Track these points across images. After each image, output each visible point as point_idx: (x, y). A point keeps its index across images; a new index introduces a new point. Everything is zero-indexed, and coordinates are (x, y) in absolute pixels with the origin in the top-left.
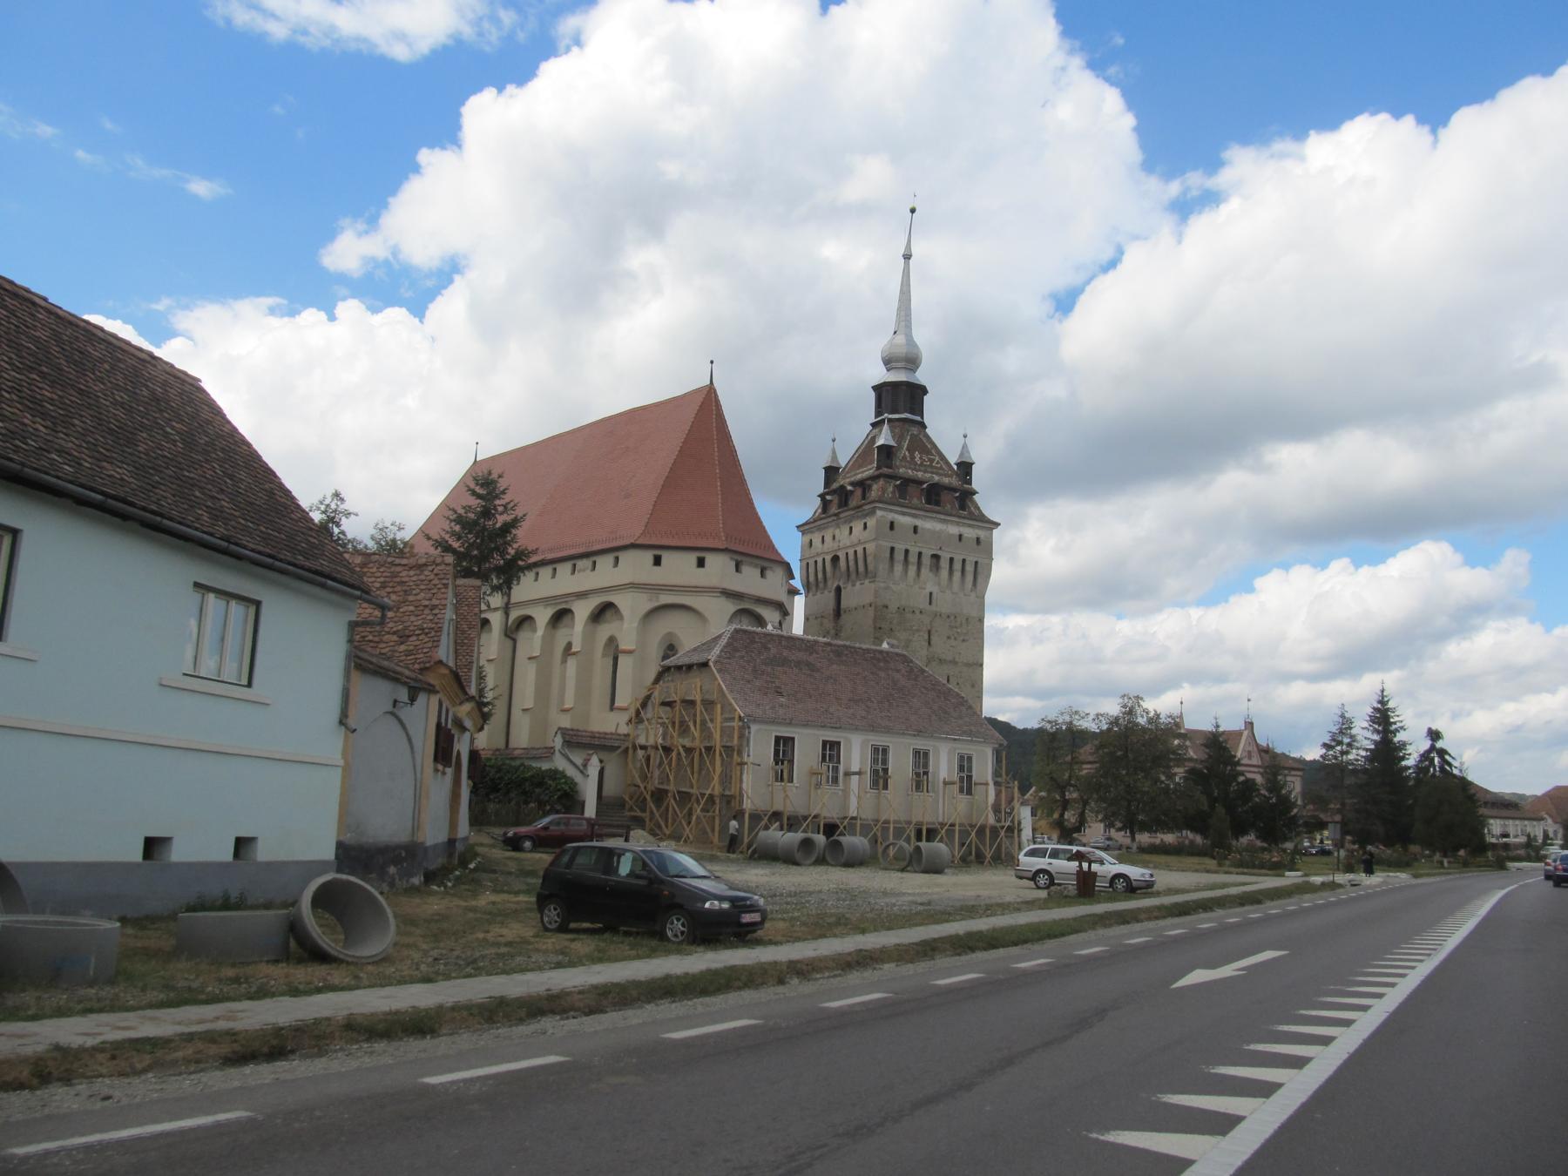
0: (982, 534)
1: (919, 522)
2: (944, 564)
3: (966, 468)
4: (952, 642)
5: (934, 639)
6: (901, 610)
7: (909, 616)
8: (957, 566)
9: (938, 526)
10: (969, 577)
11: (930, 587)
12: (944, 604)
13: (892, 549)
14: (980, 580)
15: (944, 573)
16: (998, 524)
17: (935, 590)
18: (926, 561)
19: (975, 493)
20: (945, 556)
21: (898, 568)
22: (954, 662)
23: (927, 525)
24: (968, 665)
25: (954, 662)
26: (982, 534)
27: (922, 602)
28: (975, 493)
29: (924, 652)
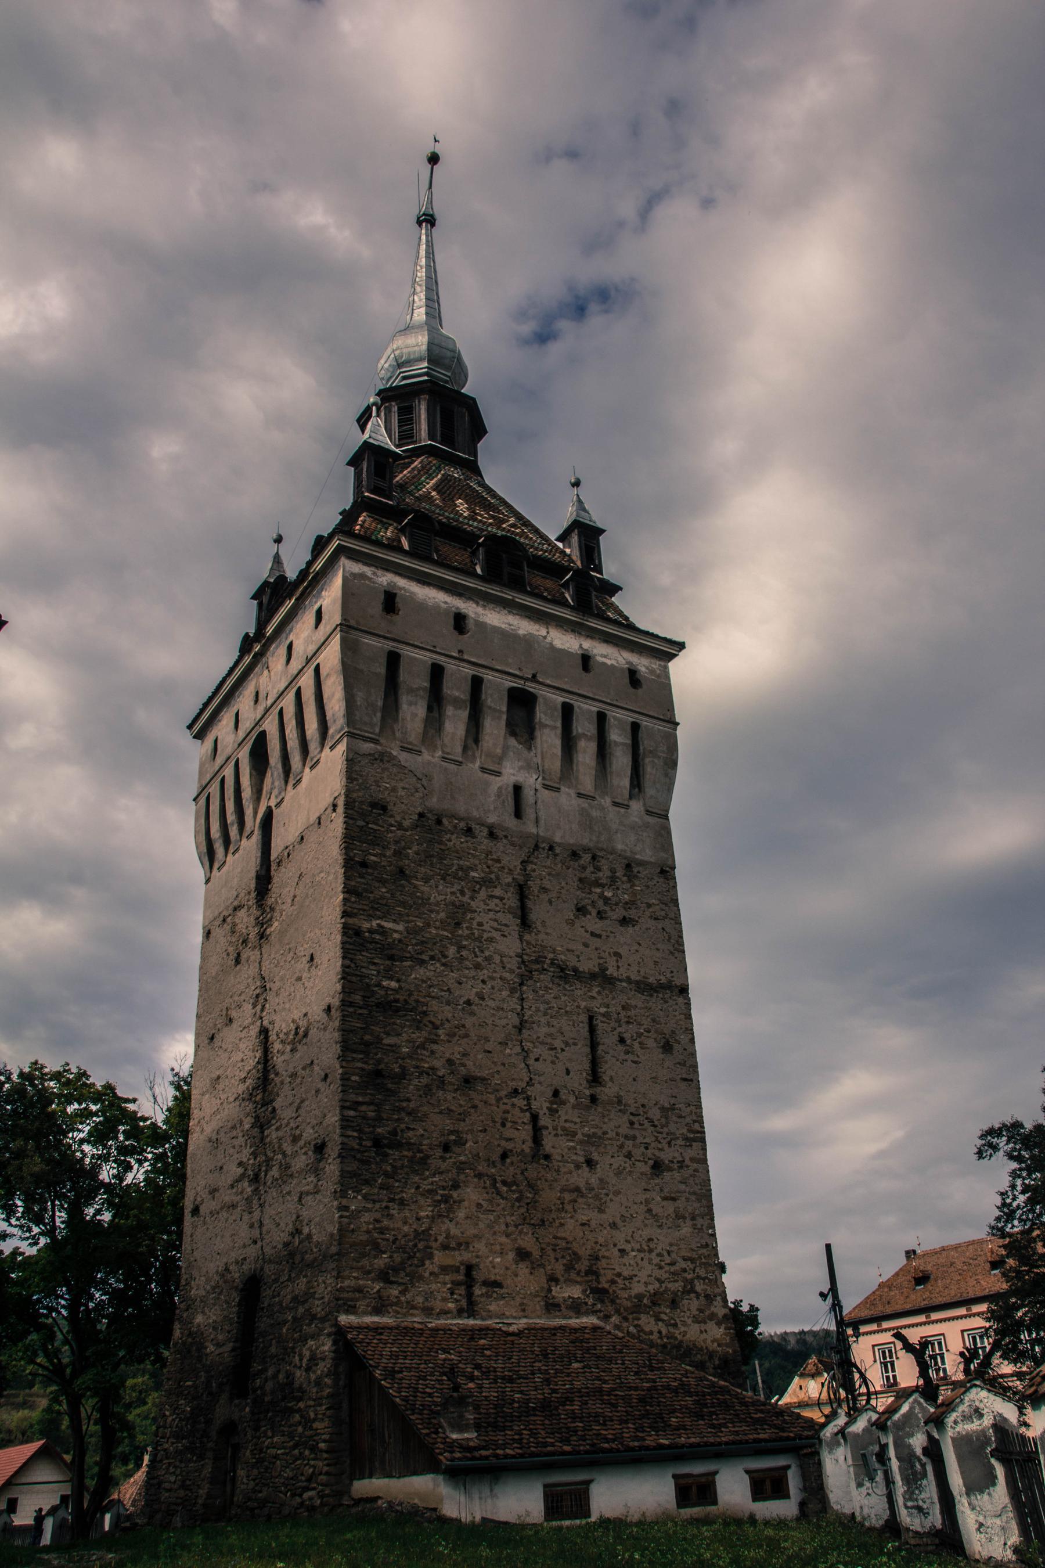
0: (643, 664)
1: (470, 609)
2: (547, 717)
3: (587, 534)
4: (592, 923)
5: (538, 912)
6: (431, 823)
7: (456, 841)
8: (585, 727)
9: (525, 627)
10: (621, 761)
11: (511, 773)
12: (559, 815)
13: (393, 660)
14: (651, 769)
15: (549, 739)
16: (681, 646)
17: (530, 781)
18: (495, 701)
19: (614, 589)
20: (549, 701)
21: (413, 712)
22: (602, 978)
23: (495, 618)
24: (644, 987)
25: (602, 978)
26: (643, 664)
27: (499, 815)
28: (614, 589)
29: (510, 945)
